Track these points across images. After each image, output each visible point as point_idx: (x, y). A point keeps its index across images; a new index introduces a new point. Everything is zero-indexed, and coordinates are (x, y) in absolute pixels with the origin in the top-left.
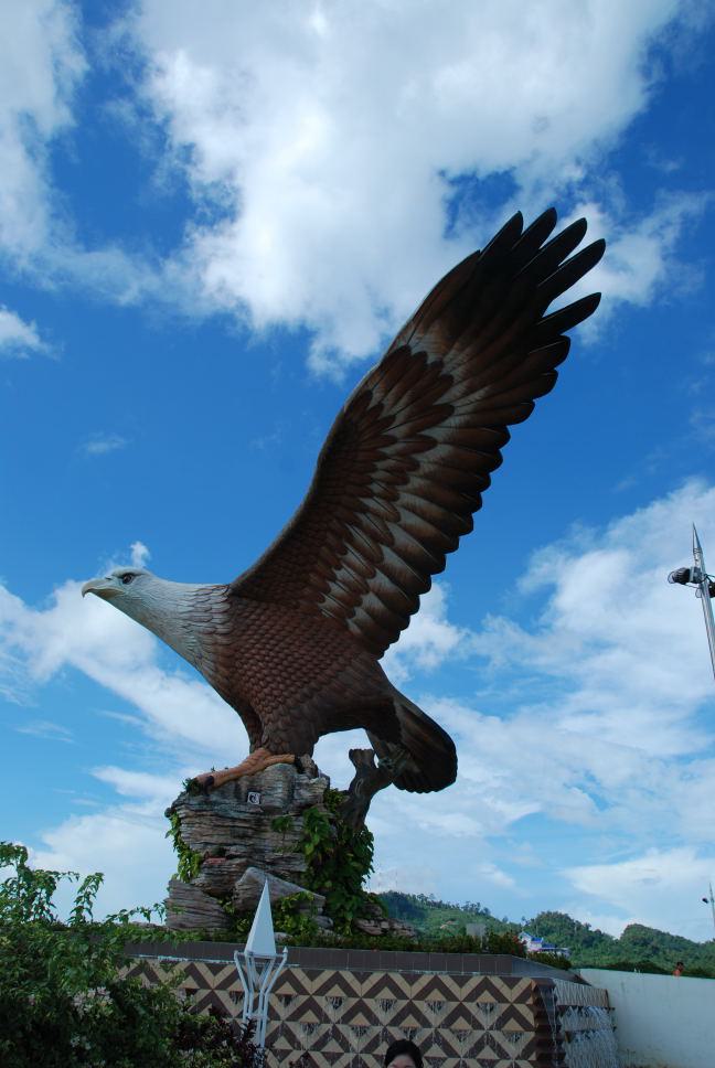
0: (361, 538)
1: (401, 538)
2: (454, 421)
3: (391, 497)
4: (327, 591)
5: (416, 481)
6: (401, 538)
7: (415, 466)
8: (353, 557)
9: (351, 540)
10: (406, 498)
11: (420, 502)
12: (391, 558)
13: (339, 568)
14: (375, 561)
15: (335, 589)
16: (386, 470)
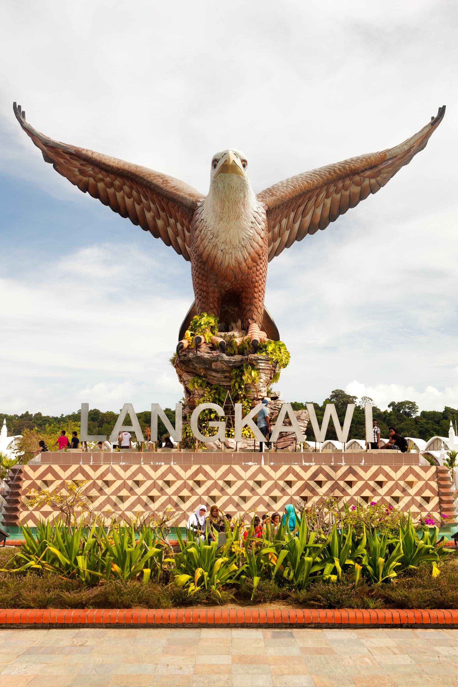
0: (301, 208)
1: (308, 218)
2: (373, 181)
3: (327, 197)
4: (274, 227)
5: (338, 197)
6: (308, 218)
7: (346, 190)
8: (292, 215)
9: (299, 206)
10: (328, 201)
11: (328, 206)
12: (297, 226)
13: (286, 218)
14: (294, 221)
15: (276, 230)
16: (343, 185)
